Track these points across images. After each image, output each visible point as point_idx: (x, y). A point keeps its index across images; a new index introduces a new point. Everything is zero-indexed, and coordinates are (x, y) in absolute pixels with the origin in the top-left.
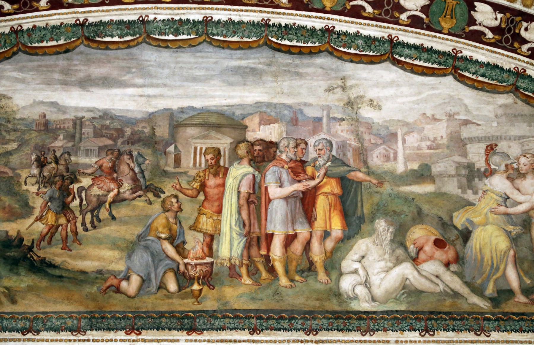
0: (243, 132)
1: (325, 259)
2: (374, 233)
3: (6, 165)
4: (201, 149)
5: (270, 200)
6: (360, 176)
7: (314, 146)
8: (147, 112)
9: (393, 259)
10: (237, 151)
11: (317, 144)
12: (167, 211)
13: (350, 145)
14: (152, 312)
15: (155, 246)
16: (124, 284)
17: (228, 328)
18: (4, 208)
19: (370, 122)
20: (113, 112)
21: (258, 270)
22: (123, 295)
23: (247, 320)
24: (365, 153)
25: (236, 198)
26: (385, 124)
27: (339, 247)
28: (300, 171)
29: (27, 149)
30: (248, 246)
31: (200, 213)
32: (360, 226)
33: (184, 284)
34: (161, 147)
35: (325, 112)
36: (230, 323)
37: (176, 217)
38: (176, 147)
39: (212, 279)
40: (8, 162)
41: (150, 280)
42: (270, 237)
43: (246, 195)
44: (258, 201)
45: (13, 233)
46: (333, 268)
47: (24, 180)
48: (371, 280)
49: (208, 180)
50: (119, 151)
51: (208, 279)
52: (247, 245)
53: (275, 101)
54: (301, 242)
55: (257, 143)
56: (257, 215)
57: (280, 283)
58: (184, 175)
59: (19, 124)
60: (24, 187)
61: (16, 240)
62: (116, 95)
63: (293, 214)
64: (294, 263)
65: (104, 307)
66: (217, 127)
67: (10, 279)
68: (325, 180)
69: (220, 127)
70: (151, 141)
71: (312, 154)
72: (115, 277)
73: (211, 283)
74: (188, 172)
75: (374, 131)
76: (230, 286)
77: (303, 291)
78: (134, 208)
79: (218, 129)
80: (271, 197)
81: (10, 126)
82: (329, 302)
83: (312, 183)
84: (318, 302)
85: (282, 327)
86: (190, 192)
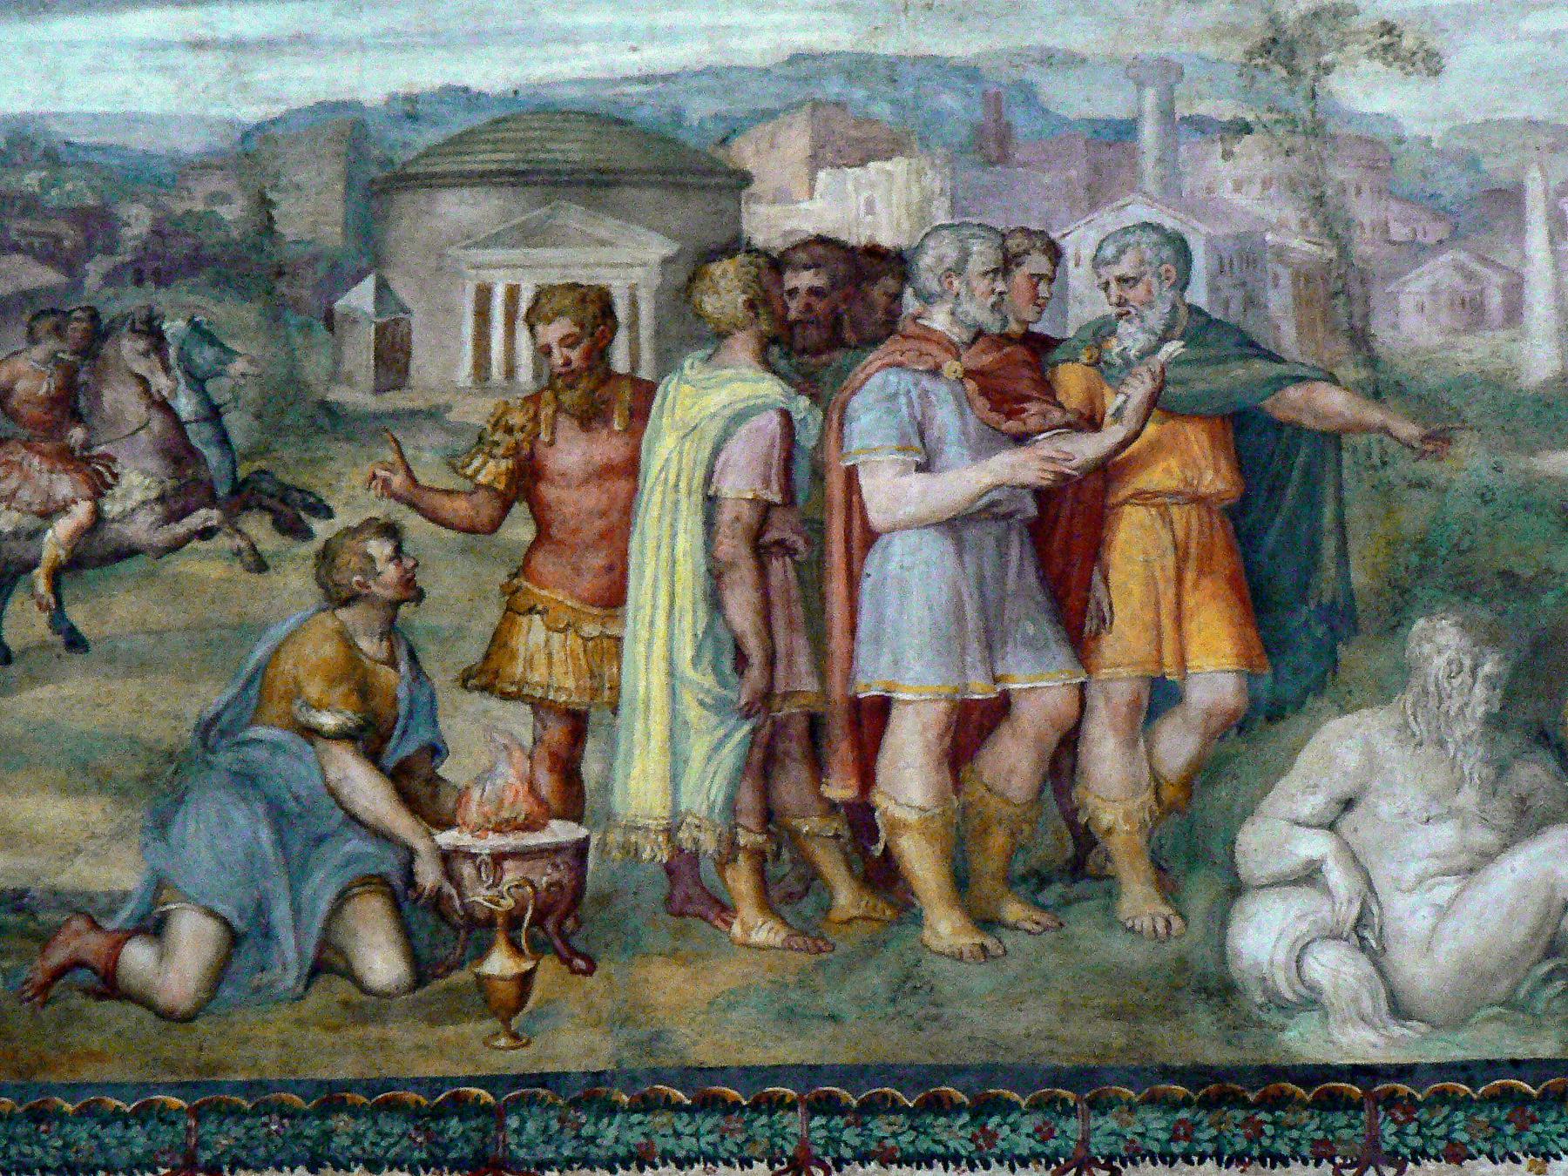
0: (726, 203)
1: (1157, 821)
2: (1404, 686)
4: (513, 293)
5: (871, 537)
6: (1334, 402)
7: (1097, 262)
8: (231, 123)
9: (1501, 810)
10: (697, 298)
11: (1110, 251)
12: (346, 603)
13: (1281, 253)
14: (284, 1086)
15: (294, 770)
16: (138, 957)
17: (667, 1156)
19: (1384, 133)
20: (57, 127)
21: (811, 878)
22: (135, 1011)
23: (764, 1119)
24: (1356, 289)
25: (699, 529)
26: (1463, 143)
27: (1228, 759)
28: (1025, 387)
30: (763, 764)
31: (515, 607)
32: (1333, 651)
33: (441, 952)
34: (306, 293)
35: (1150, 97)
36: (678, 1135)
37: (391, 631)
38: (382, 287)
39: (579, 923)
41: (267, 933)
42: (872, 718)
43: (748, 514)
44: (807, 542)
46: (1196, 857)
48: (1388, 916)
49: (551, 444)
50: (94, 316)
51: (560, 924)
52: (758, 755)
53: (889, 46)
54: (1031, 733)
55: (802, 256)
56: (807, 609)
57: (927, 934)
58: (428, 425)
62: (73, 45)
63: (992, 595)
64: (998, 840)
65: (43, 1064)
66: (595, 184)
68: (1151, 429)
69: (608, 185)
70: (253, 265)
71: (1084, 300)
72: (95, 926)
73: (578, 943)
74: (449, 408)
75: (1407, 181)
76: (673, 955)
77: (1045, 977)
78: (178, 590)
79: (595, 192)
80: (876, 518)
82: (1174, 1024)
83: (1088, 448)
84: (1116, 1024)
85: (940, 1149)
86: (459, 508)
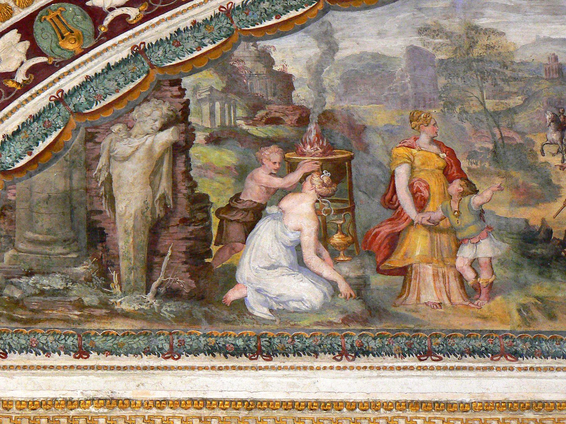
3: (511, 128)
18: (517, 188)
29: (538, 104)
40: (513, 123)
45: (536, 223)
47: (540, 149)
59: (520, 70)
60: (541, 159)
61: (542, 233)
67: (541, 287)
81: (508, 73)
